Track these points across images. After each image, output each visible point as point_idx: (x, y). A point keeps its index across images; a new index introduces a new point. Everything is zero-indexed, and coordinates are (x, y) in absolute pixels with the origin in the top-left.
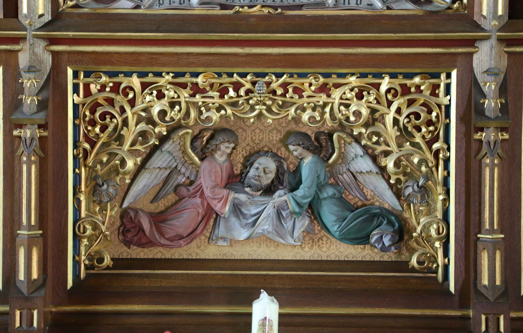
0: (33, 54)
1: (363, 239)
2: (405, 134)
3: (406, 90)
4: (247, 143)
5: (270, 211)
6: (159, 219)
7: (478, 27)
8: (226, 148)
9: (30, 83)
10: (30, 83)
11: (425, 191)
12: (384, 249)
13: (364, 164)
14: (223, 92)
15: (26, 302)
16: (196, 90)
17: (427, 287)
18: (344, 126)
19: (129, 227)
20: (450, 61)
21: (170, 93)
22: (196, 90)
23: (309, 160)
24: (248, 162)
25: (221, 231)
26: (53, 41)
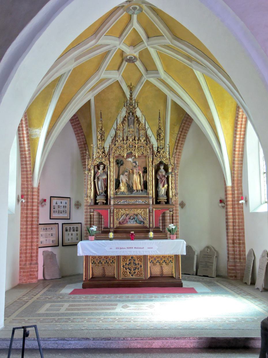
0: (112, 208)
1: (140, 224)
2: (144, 214)
3: (144, 210)
4: (130, 215)
5: (132, 221)
6: (122, 222)
7: (149, 205)
8: (128, 216)
9: (112, 210)
10: (112, 210)
11: (146, 219)
12: (142, 224)
13: (140, 217)
14: (128, 211)
15: (112, 229)
16: (126, 210)
17: (146, 228)
18: (139, 214)
19: (120, 223)
20: (147, 208)
21: (123, 211)
22: (126, 210)
23: (136, 216)
24: (130, 217)
25: (128, 223)
26: (114, 206)
